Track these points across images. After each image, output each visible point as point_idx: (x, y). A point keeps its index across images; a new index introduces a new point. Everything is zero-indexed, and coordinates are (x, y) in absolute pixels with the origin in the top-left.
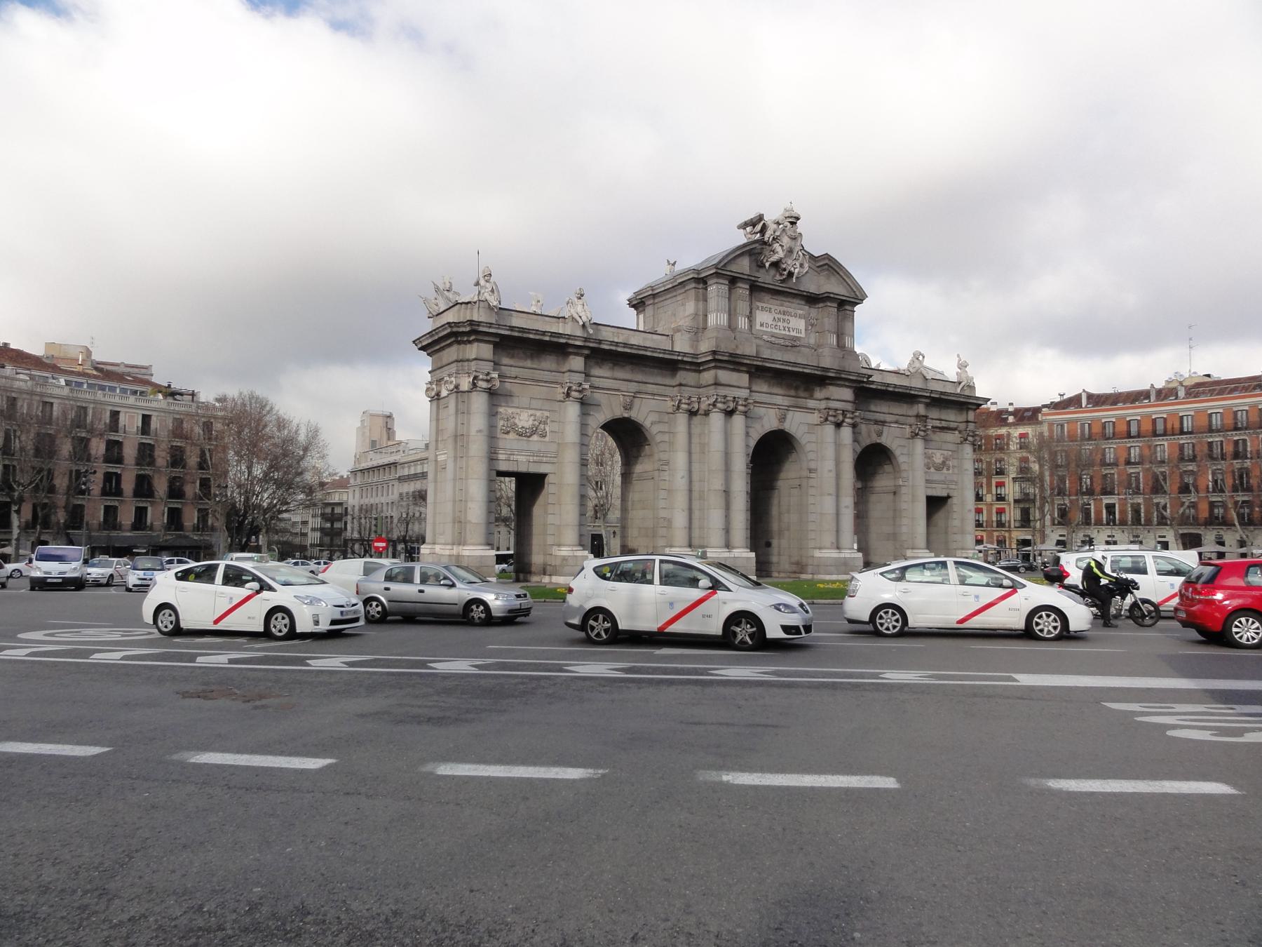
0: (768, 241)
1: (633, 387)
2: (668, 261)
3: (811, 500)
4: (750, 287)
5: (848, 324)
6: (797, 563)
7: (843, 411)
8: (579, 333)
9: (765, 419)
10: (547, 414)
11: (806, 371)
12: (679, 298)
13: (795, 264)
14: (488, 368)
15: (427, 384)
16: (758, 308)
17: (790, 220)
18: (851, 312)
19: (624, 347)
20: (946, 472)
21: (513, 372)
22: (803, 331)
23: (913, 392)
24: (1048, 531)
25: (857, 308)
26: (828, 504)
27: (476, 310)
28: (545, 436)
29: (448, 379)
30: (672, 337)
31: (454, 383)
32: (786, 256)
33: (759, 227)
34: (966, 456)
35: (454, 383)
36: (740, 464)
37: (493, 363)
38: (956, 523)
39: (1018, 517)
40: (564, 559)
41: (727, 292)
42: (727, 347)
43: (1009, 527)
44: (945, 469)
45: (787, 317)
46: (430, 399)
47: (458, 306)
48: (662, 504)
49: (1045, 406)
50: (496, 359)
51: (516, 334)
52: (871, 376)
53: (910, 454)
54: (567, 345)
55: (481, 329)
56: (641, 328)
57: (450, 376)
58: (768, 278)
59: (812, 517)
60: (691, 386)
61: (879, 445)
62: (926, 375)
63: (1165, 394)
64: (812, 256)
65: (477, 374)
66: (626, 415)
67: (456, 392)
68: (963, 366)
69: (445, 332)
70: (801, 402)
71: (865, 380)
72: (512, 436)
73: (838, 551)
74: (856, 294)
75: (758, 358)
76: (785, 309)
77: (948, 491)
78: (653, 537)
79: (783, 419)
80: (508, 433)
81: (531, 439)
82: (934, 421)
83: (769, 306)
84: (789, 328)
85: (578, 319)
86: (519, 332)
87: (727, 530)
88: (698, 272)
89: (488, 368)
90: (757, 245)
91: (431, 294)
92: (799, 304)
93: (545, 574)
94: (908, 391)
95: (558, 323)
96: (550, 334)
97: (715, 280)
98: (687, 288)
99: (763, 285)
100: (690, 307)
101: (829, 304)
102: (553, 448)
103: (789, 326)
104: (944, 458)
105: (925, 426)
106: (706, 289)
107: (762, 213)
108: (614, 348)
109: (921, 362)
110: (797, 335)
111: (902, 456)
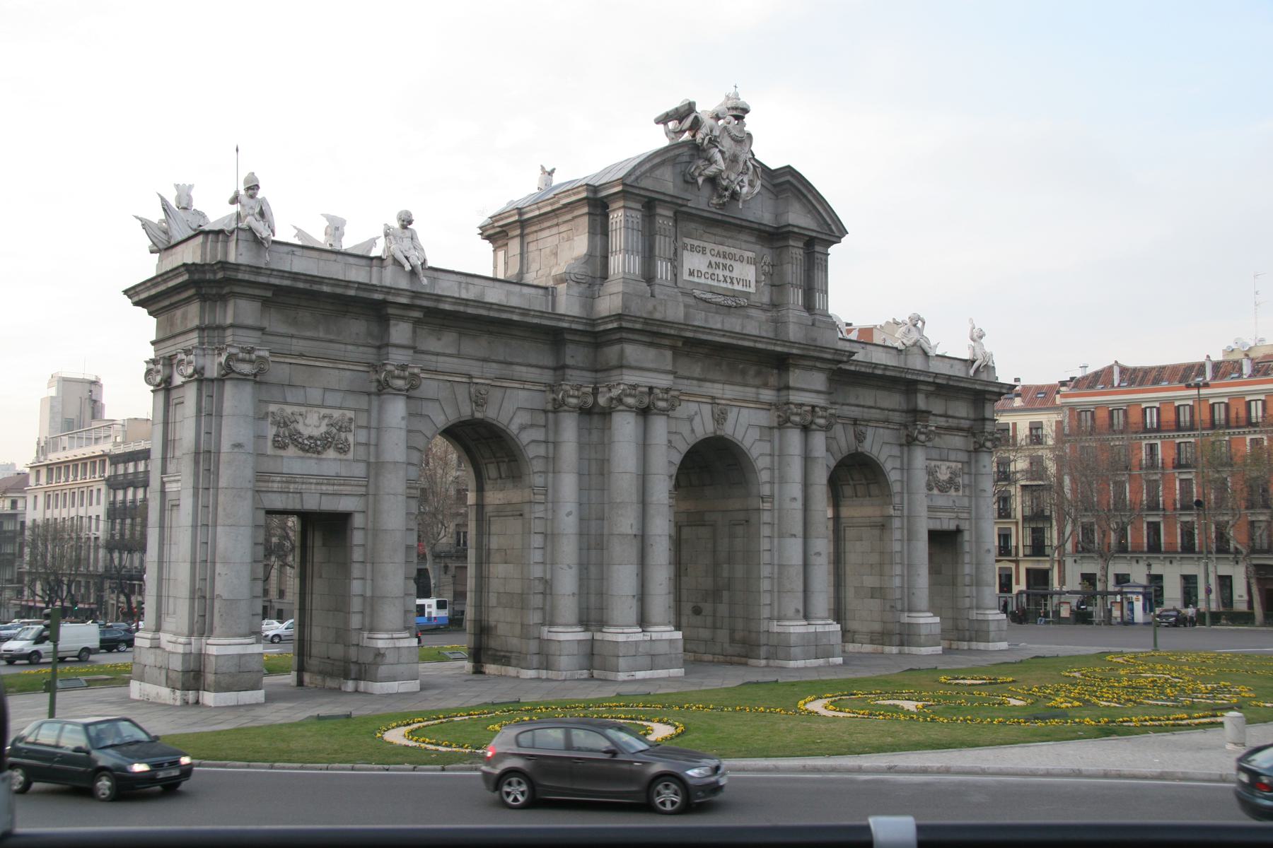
0: (702, 143)
1: (493, 369)
2: (543, 168)
3: (765, 544)
4: (675, 213)
5: (818, 275)
6: (744, 642)
7: (813, 407)
8: (403, 283)
9: (697, 420)
10: (350, 414)
11: (759, 346)
12: (563, 228)
13: (742, 181)
14: (251, 340)
15: (147, 362)
16: (685, 247)
17: (735, 113)
18: (823, 257)
19: (477, 307)
21: (298, 345)
23: (909, 376)
24: (1069, 562)
25: (832, 250)
26: (794, 551)
27: (232, 245)
28: (345, 452)
29: (183, 356)
30: (553, 292)
31: (194, 364)
32: (726, 169)
33: (688, 122)
34: (984, 471)
35: (194, 364)
36: (661, 490)
37: (259, 334)
38: (967, 569)
39: (1029, 542)
40: (379, 654)
41: (640, 221)
42: (640, 309)
43: (1017, 554)
44: (953, 489)
45: (728, 262)
46: (152, 388)
47: (200, 239)
48: (537, 556)
49: (1063, 384)
50: (265, 324)
51: (301, 285)
52: (853, 353)
53: (906, 468)
54: (385, 303)
55: (240, 276)
56: (501, 276)
57: (187, 352)
58: (702, 200)
59: (765, 571)
60: (582, 369)
61: (862, 454)
62: (928, 350)
63: (1224, 370)
64: (764, 168)
65: (234, 351)
66: (478, 415)
67: (196, 380)
68: (977, 337)
69: (180, 280)
70: (750, 392)
71: (845, 359)
72: (292, 451)
73: (805, 623)
74: (832, 231)
75: (688, 325)
76: (725, 249)
78: (522, 608)
79: (720, 418)
80: (284, 447)
81: (323, 456)
83: (702, 244)
84: (732, 279)
85: (404, 261)
86: (306, 281)
87: (642, 597)
88: (594, 189)
89: (251, 340)
90: (686, 149)
91: (157, 216)
92: (745, 241)
93: (346, 676)
94: (903, 375)
95: (371, 267)
96: (356, 286)
97: (621, 204)
98: (576, 213)
99: (694, 211)
100: (580, 244)
101: (791, 243)
104: (951, 473)
105: (926, 427)
106: (607, 216)
107: (692, 100)
108: (461, 309)
109: (920, 331)
110: (744, 289)
111: (893, 471)
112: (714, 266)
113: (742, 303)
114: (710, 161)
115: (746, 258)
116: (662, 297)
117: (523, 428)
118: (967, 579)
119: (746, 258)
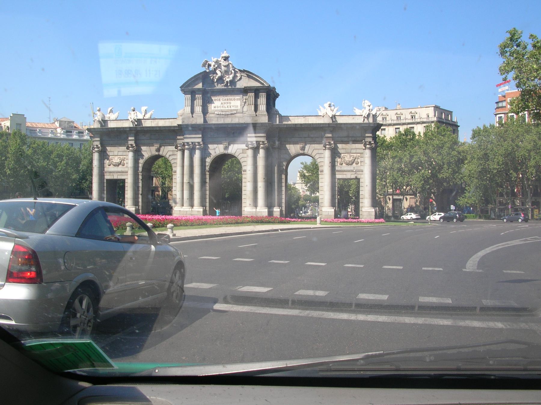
20: (355, 165)
22: (239, 106)
28: (124, 165)
44: (354, 163)
45: (229, 101)
66: (157, 153)
72: (112, 166)
77: (356, 175)
80: (110, 165)
82: (343, 138)
83: (218, 98)
94: (312, 126)
102: (126, 169)
103: (230, 105)
108: (143, 129)
110: (236, 108)
112: (223, 103)
113: (233, 113)
114: (217, 74)
115: (236, 99)
116: (196, 117)
117: (170, 156)
118: (361, 197)
119: (236, 99)
